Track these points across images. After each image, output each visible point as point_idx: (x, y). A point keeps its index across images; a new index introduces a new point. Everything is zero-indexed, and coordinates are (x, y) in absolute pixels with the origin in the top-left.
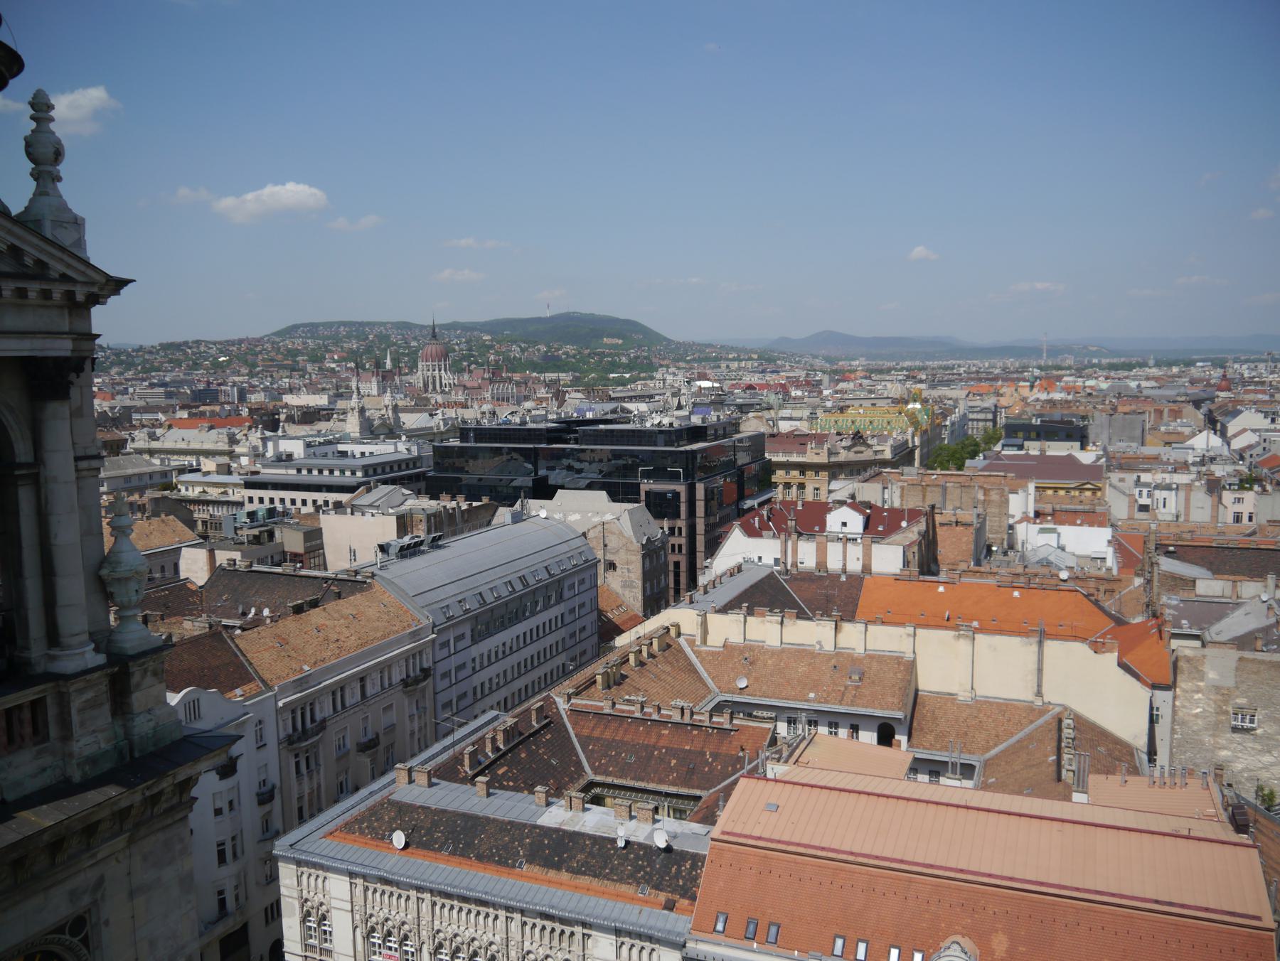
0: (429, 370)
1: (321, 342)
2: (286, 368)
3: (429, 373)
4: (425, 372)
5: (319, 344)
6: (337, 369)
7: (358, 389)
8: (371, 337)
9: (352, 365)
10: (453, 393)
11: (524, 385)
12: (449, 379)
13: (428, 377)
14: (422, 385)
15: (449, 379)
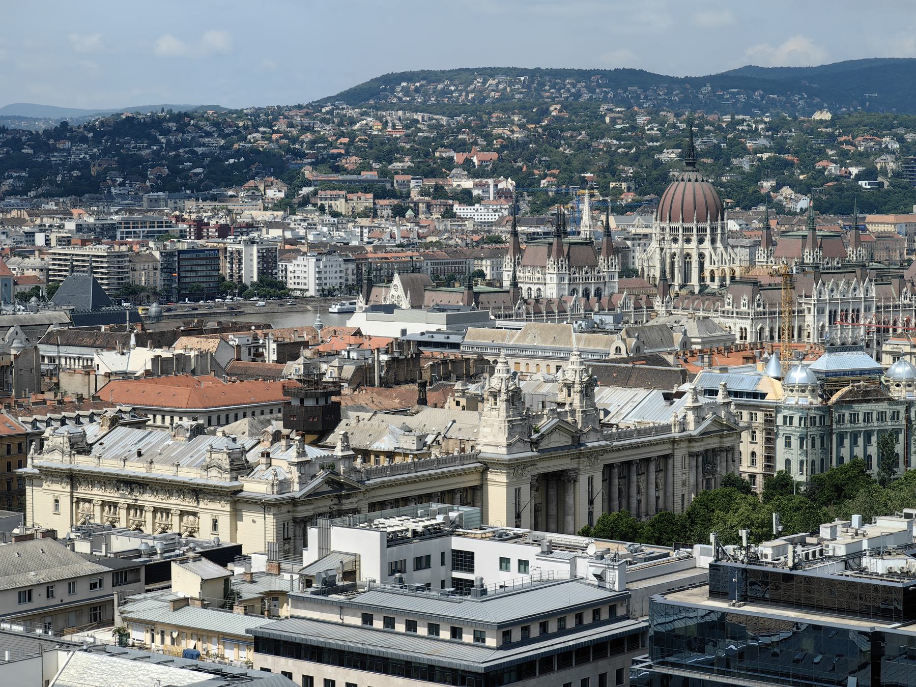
0: (675, 240)
1: (444, 120)
2: (366, 190)
3: (676, 248)
4: (666, 245)
5: (438, 126)
6: (476, 192)
7: (515, 283)
8: (554, 109)
9: (508, 184)
10: (728, 299)
11: (896, 281)
12: (722, 261)
13: (673, 256)
14: (658, 275)
15: (722, 261)
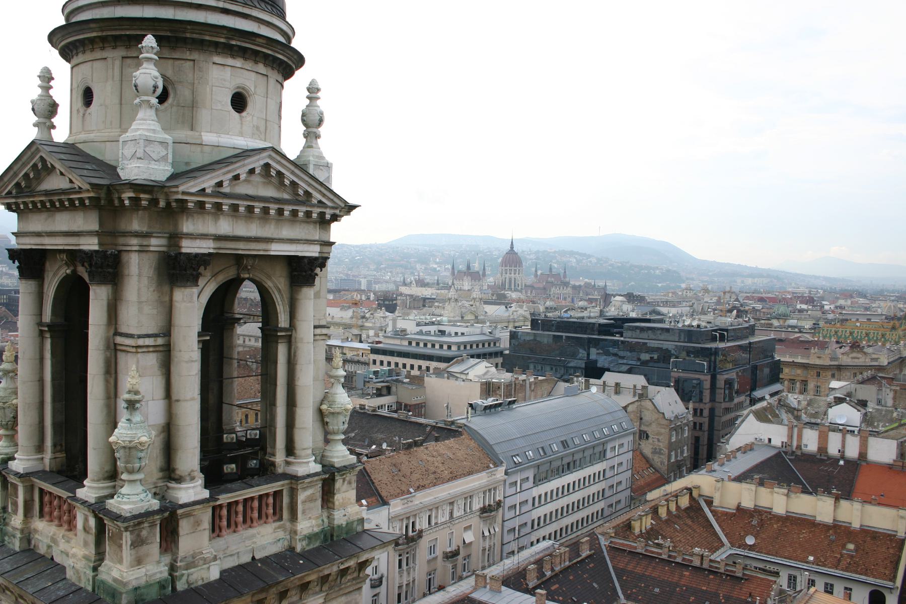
6: (438, 269)
